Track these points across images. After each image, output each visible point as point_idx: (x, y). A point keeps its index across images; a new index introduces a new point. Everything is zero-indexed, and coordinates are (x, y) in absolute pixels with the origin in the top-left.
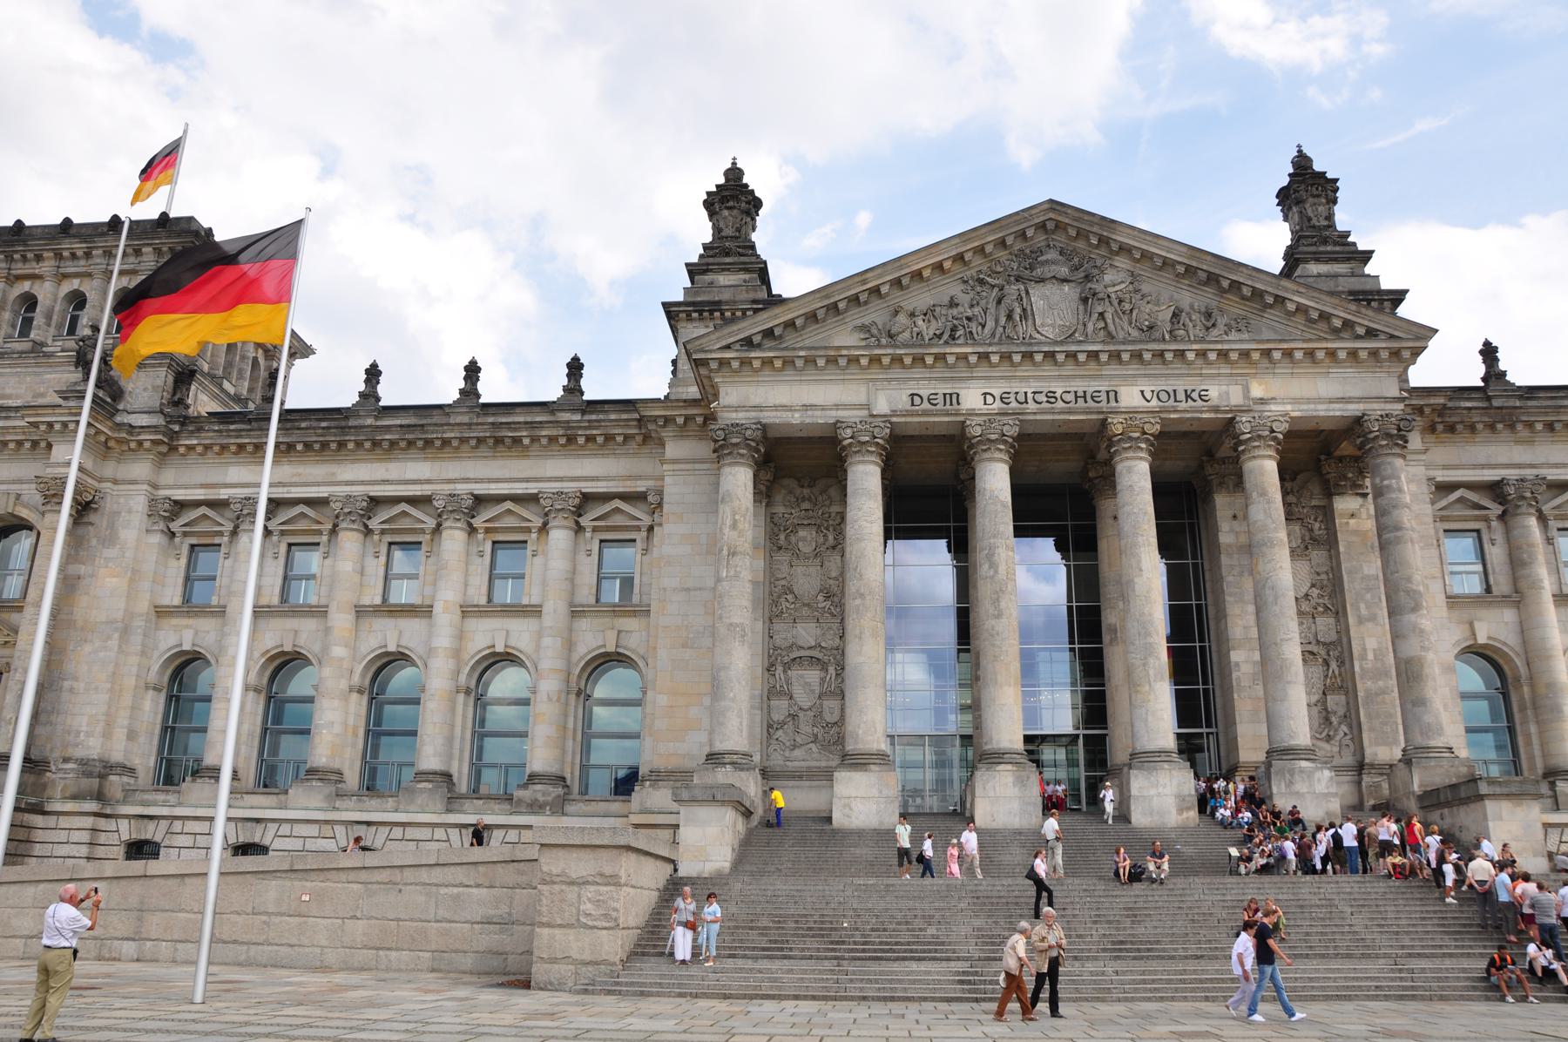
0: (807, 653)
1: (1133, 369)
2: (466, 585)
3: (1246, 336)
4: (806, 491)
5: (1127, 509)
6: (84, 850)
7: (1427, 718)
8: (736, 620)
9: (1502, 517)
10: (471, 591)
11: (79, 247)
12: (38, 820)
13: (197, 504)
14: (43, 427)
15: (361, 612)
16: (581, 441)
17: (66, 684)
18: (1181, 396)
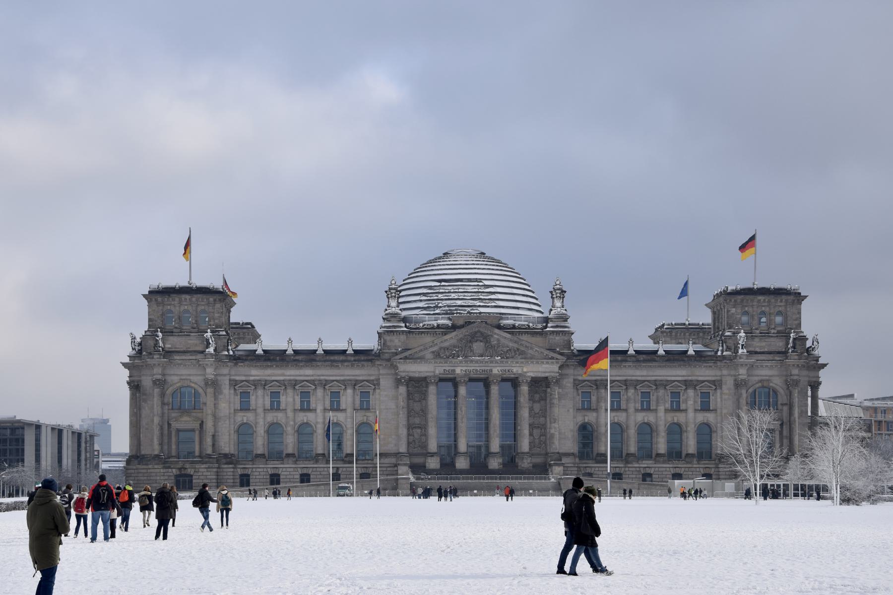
0: (417, 425)
1: (496, 365)
2: (324, 404)
3: (523, 356)
4: (417, 385)
5: (492, 398)
6: (232, 477)
7: (554, 447)
8: (404, 423)
9: (597, 388)
10: (326, 405)
11: (188, 297)
12: (219, 470)
13: (243, 381)
14: (205, 365)
15: (295, 410)
16: (355, 366)
17: (217, 434)
18: (507, 371)
